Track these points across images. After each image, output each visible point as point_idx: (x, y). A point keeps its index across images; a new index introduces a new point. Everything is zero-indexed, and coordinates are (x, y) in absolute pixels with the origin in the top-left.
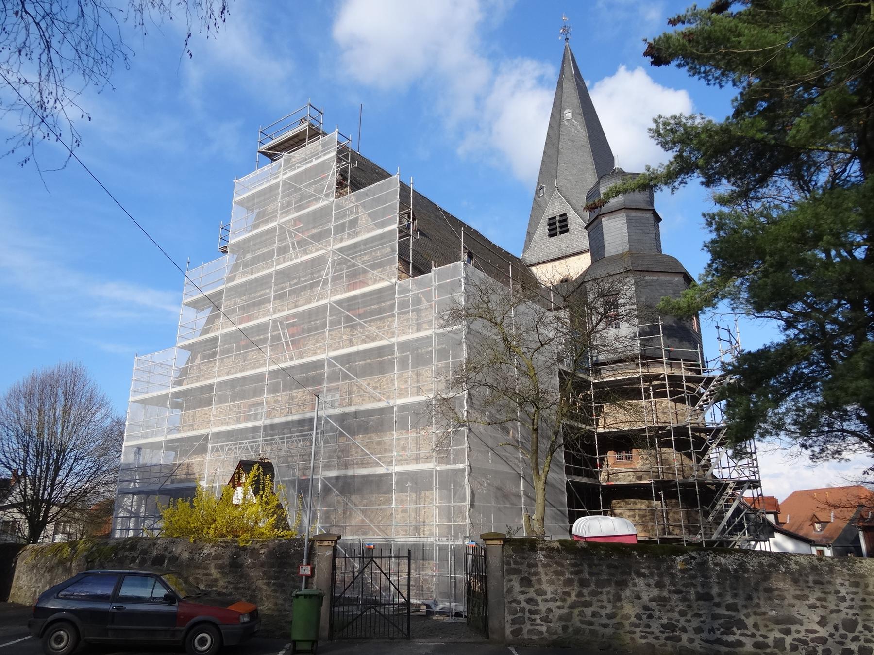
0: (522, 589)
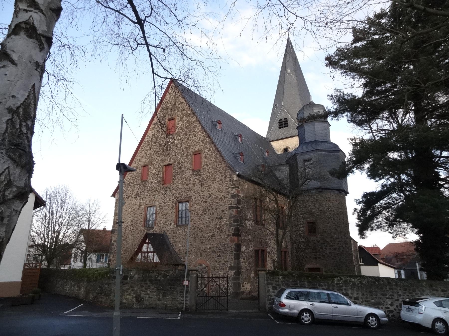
0: (273, 291)
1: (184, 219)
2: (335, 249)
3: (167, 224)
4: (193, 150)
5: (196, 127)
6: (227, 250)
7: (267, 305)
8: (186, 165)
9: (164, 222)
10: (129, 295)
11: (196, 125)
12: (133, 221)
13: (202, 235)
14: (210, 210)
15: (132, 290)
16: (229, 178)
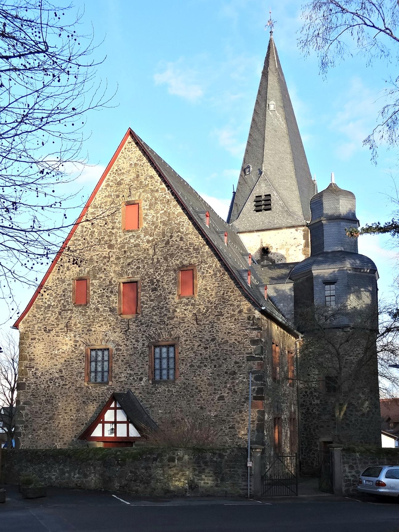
1: (165, 372)
3: (134, 379)
4: (178, 262)
5: (183, 225)
6: (245, 420)
7: (343, 488)
8: (166, 286)
9: (128, 376)
10: (179, 480)
11: (183, 222)
12: (63, 371)
13: (201, 397)
14: (214, 360)
15: (183, 475)
16: (246, 313)
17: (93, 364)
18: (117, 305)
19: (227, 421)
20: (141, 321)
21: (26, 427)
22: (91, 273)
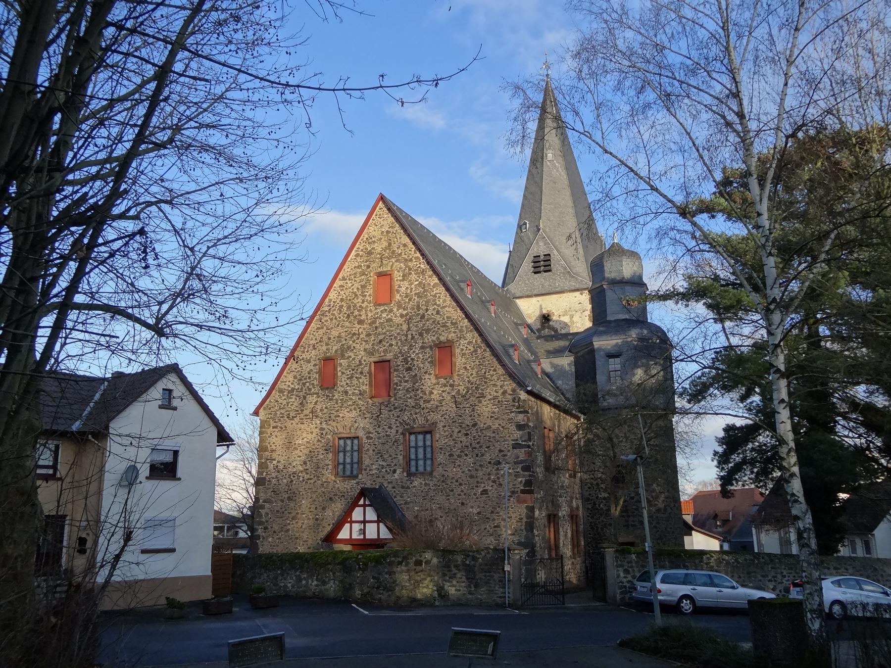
1: (421, 463)
2: (659, 510)
3: (386, 471)
4: (434, 338)
5: (439, 297)
9: (380, 468)
12: (308, 463)
14: (475, 448)
16: (510, 395)
17: (341, 455)
18: (368, 387)
19: (492, 518)
20: (394, 405)
21: (266, 528)
22: (339, 352)
